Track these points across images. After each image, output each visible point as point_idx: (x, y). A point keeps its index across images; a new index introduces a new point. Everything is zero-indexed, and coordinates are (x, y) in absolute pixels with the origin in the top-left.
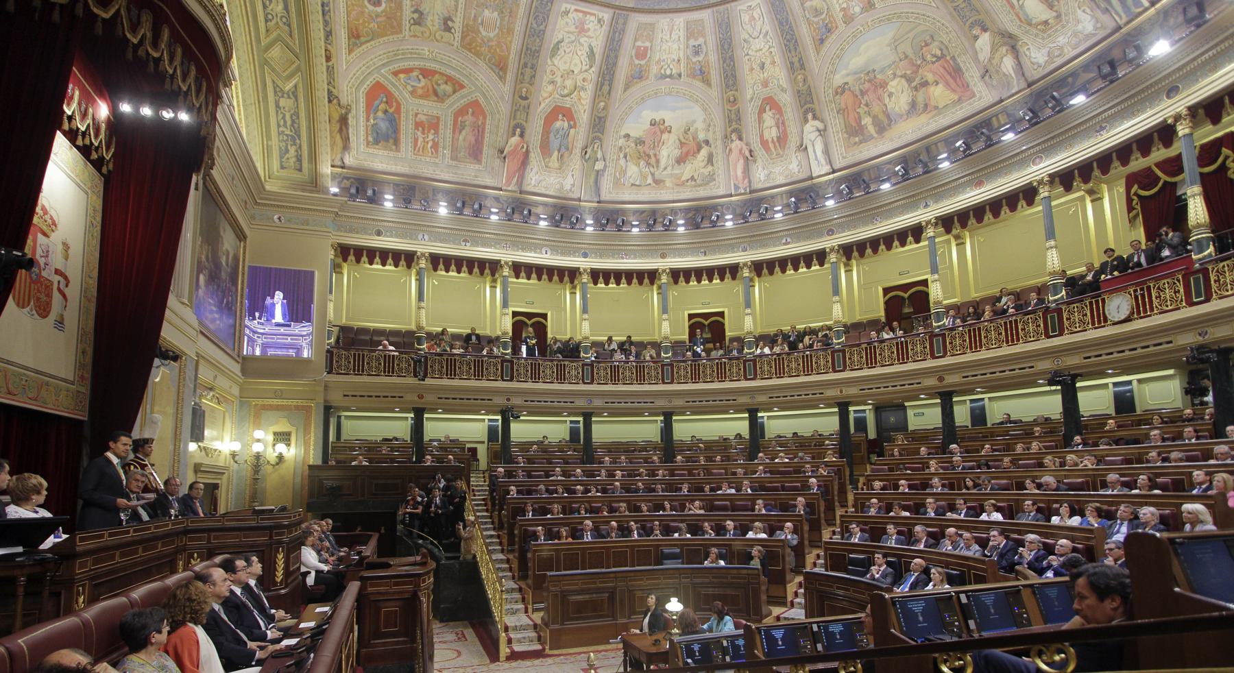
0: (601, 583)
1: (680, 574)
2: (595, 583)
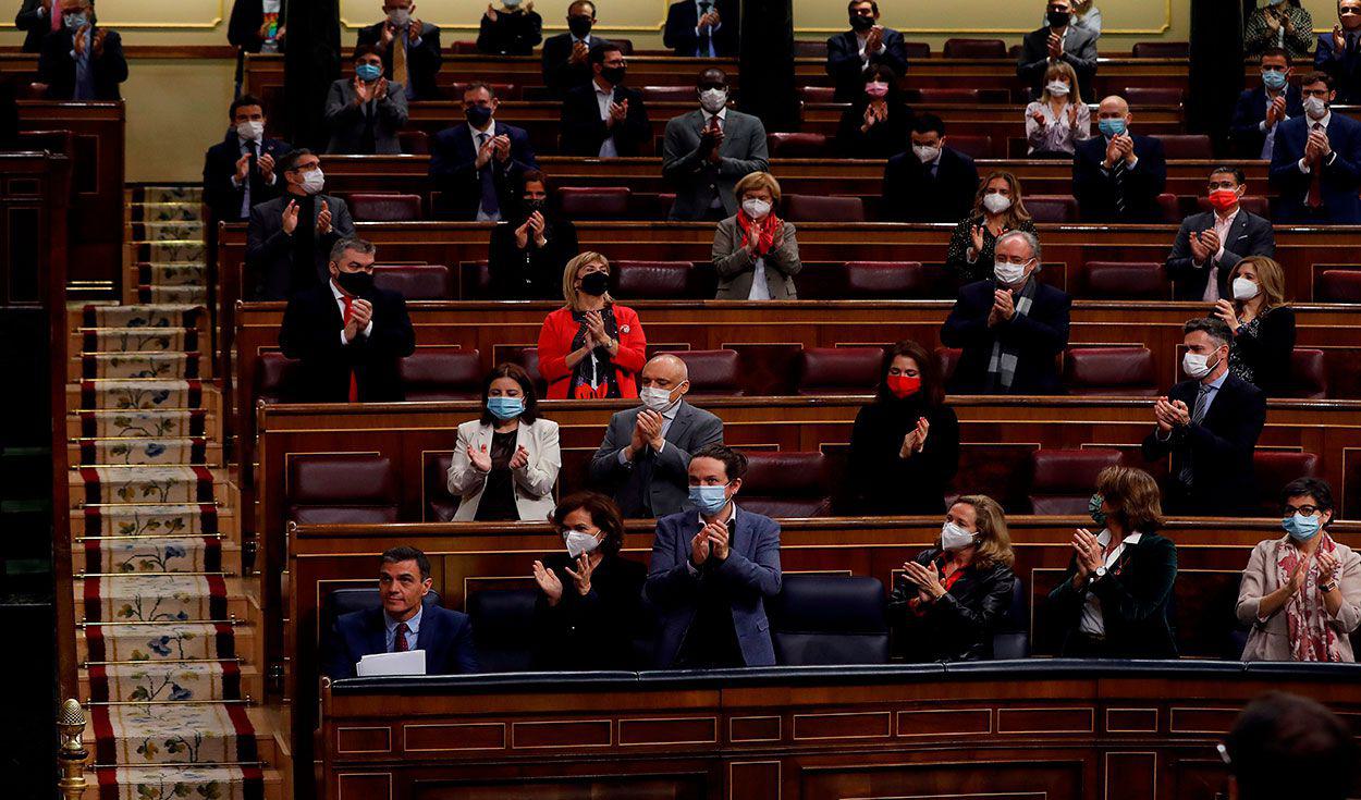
0: (631, 732)
1: (1101, 703)
2: (601, 733)
